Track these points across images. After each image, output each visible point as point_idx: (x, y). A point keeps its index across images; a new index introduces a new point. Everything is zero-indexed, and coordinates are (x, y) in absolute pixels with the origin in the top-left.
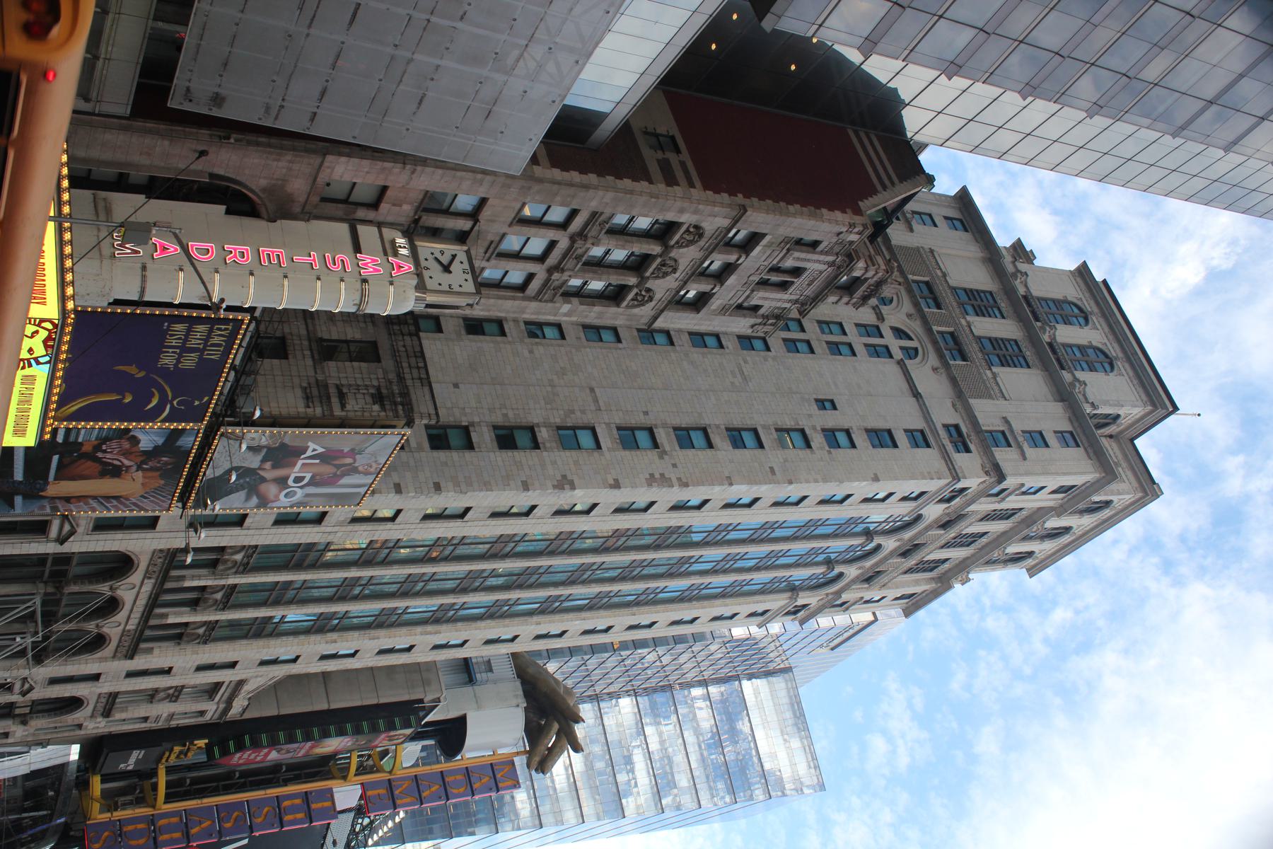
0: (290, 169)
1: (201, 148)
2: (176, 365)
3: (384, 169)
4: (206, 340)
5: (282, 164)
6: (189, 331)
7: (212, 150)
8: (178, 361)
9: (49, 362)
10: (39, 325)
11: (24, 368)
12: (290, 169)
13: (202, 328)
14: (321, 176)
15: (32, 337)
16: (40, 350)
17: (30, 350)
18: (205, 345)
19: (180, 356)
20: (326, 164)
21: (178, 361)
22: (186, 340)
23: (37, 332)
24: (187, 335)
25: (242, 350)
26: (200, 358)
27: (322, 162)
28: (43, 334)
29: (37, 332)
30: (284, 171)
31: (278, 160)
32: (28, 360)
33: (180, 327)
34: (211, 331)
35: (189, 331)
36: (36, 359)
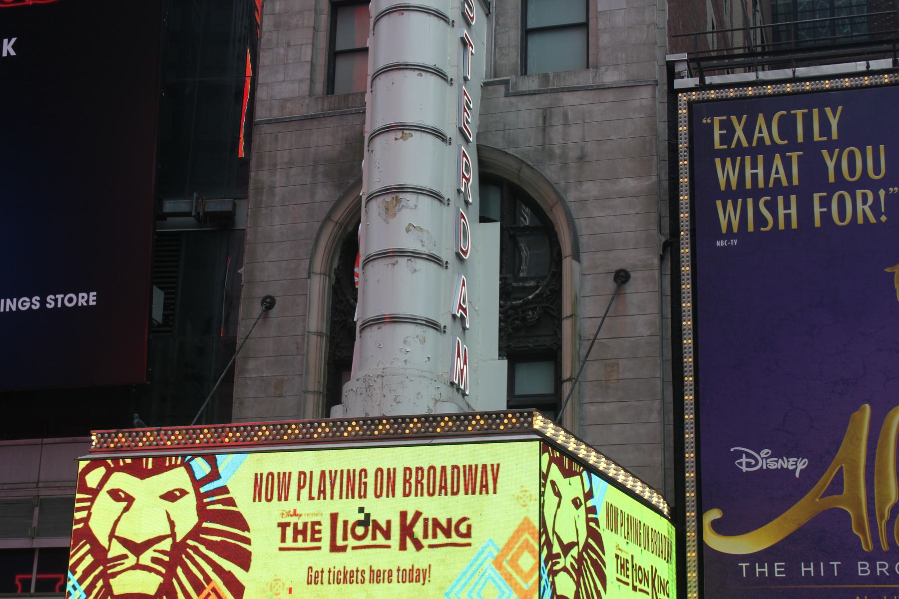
0: (290, 164)
1: (258, 309)
2: (874, 186)
3: (277, 26)
4: (769, 152)
5: (279, 178)
6: (739, 193)
7: (260, 292)
8: (865, 182)
9: (211, 460)
10: (95, 492)
11: (231, 502)
12: (290, 164)
13: (726, 174)
14: (304, 112)
15: (130, 500)
16: (177, 478)
17: (170, 497)
18: (794, 146)
19: (840, 183)
20: (276, 114)
21: (865, 182)
22: (778, 189)
23: (115, 494)
24: (756, 193)
25: (801, 71)
26: (830, 146)
27: (269, 122)
28: (120, 480)
29: (115, 494)
30: (294, 171)
31: (272, 188)
32: (200, 497)
33: (728, 216)
34: (740, 152)
35: (739, 193)
36: (197, 484)
